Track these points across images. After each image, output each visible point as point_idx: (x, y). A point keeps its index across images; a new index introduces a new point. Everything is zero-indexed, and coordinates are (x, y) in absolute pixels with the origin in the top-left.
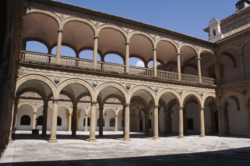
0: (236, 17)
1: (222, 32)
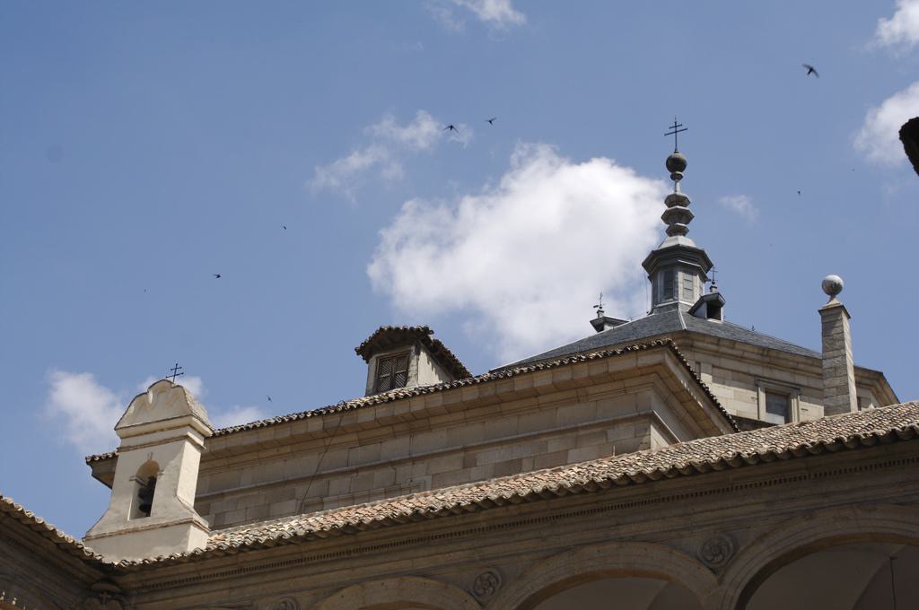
1: (202, 504)
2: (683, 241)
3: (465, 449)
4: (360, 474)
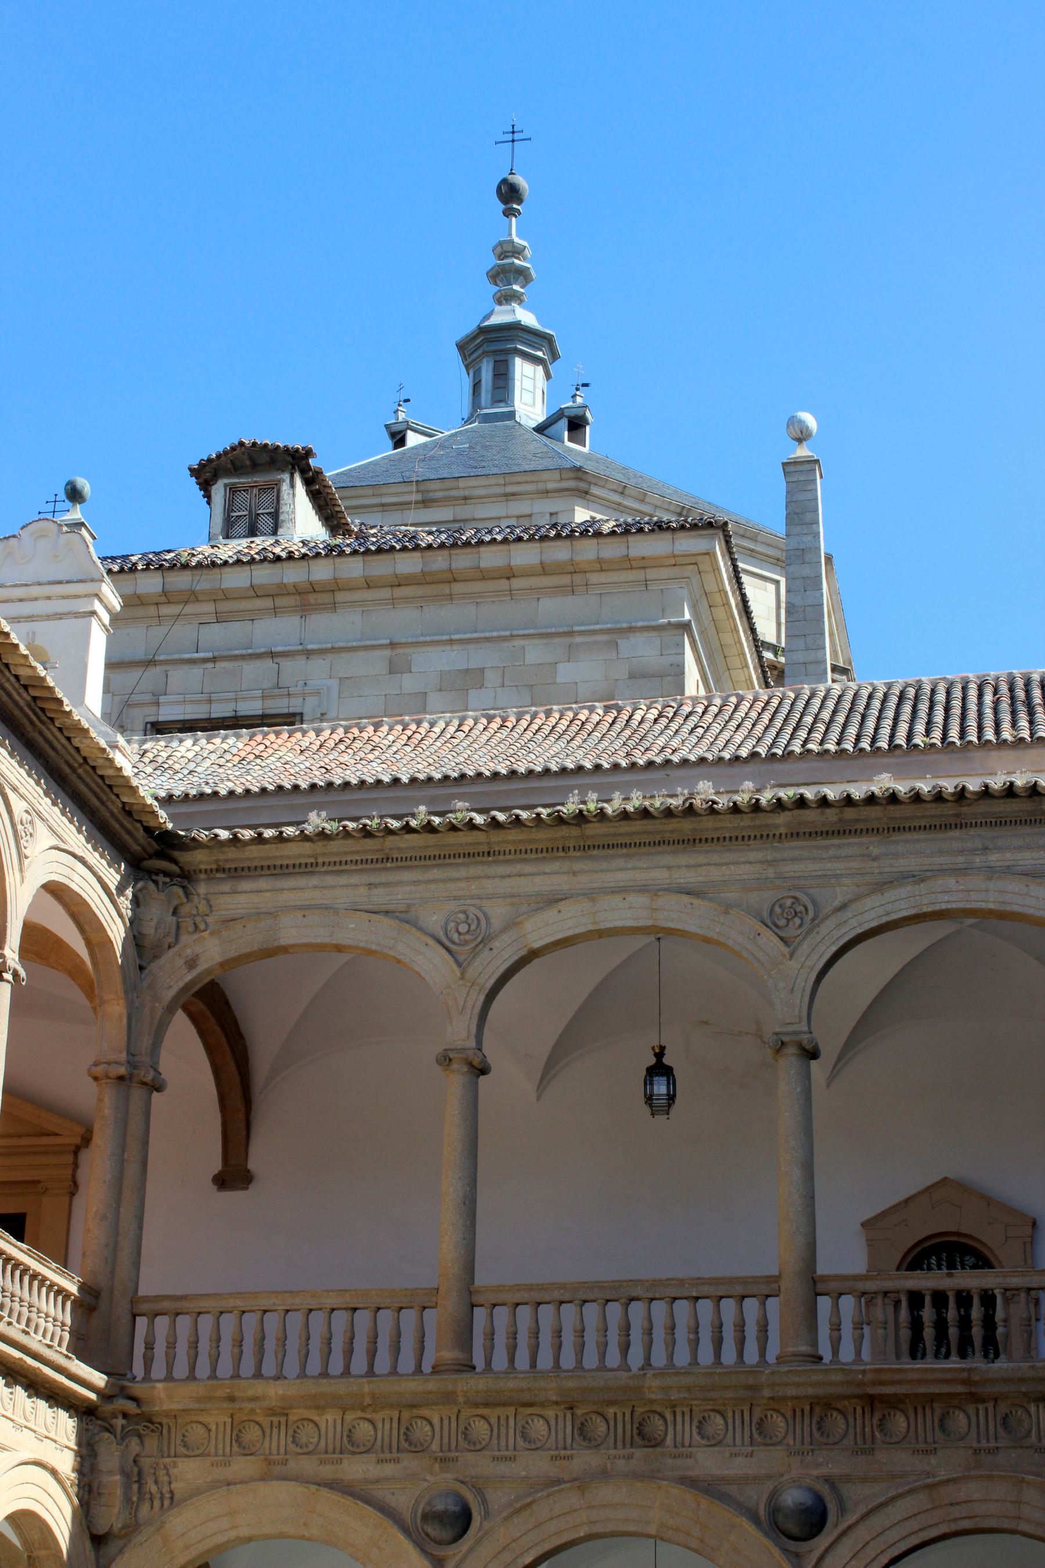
0: (192, 596)
2: (527, 317)
3: (393, 645)
4: (220, 665)
